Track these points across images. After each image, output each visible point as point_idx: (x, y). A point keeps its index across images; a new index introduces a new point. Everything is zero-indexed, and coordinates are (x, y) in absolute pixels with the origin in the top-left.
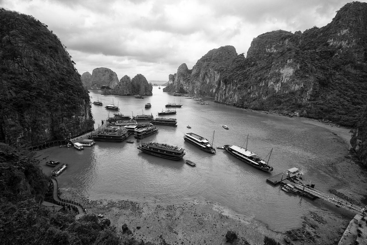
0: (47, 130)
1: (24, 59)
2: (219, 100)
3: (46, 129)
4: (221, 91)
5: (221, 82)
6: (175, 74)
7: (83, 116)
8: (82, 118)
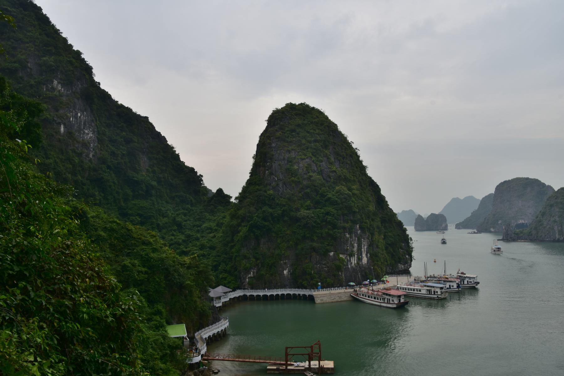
0: (287, 271)
1: (275, 163)
3: (286, 270)
7: (351, 255)
8: (347, 260)
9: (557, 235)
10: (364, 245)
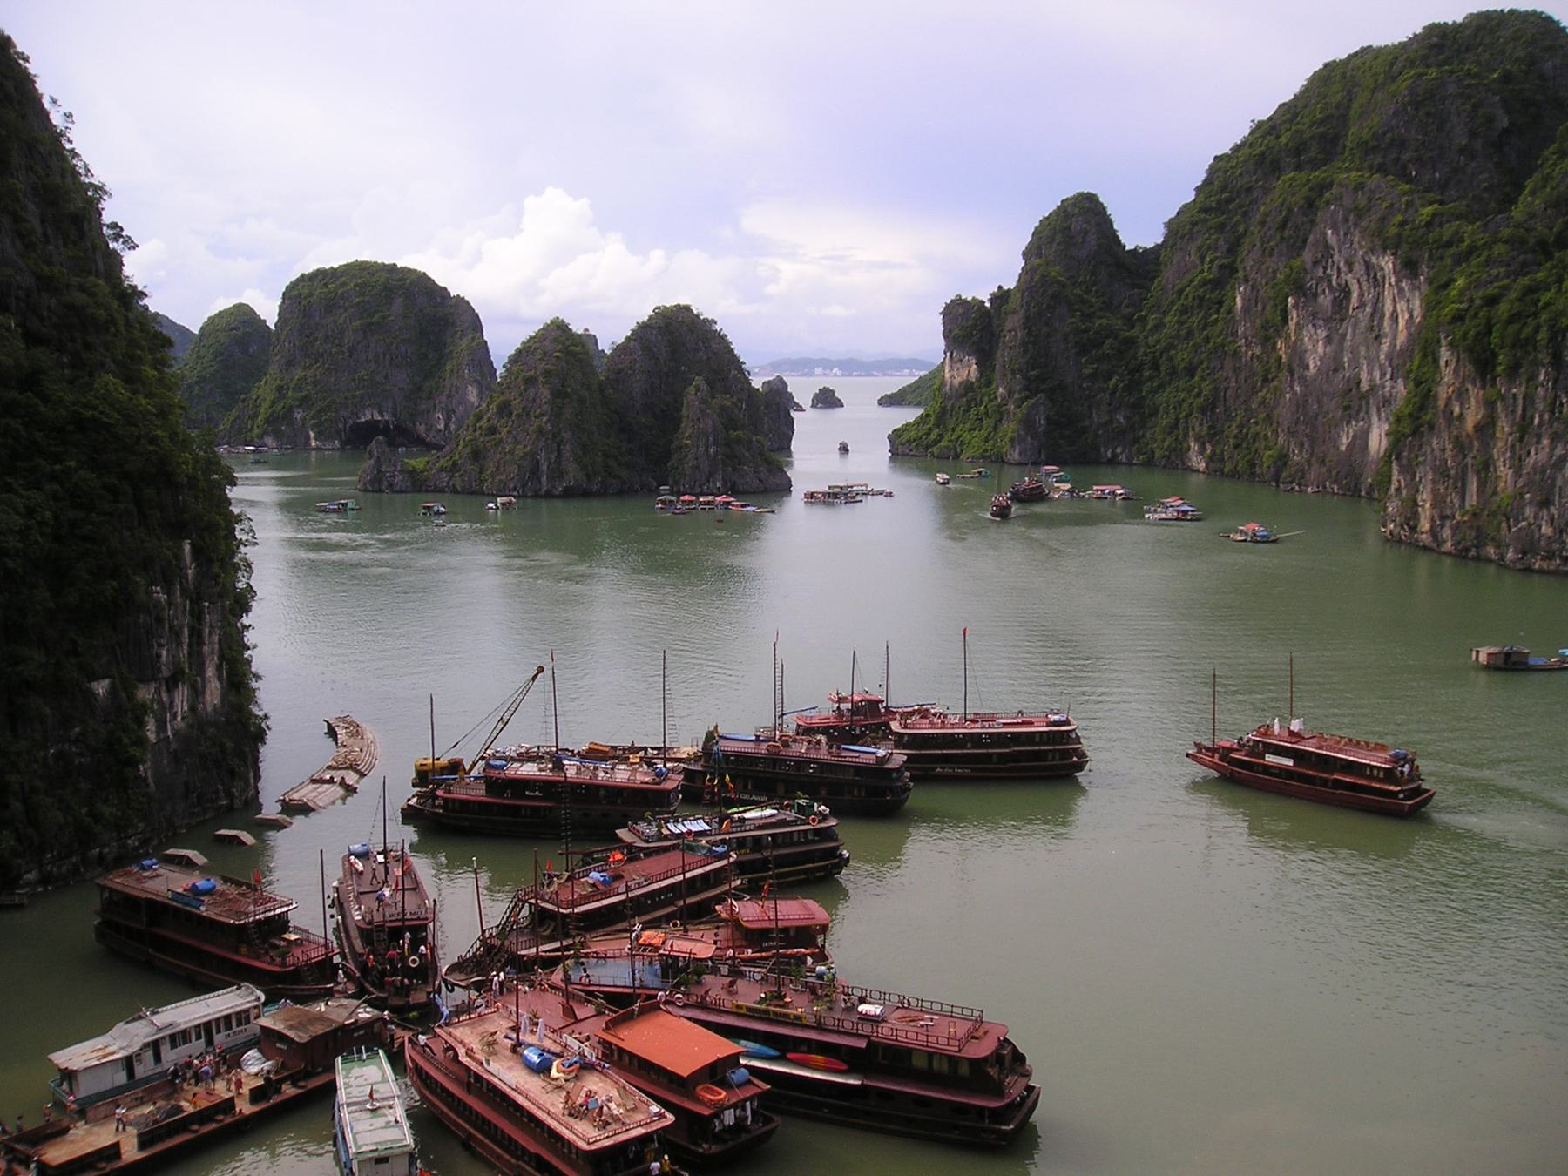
2: (1425, 525)
4: (1439, 444)
5: (1445, 354)
6: (1001, 297)
7: (172, 683)
8: (160, 702)
9: (544, 479)
10: (211, 626)
